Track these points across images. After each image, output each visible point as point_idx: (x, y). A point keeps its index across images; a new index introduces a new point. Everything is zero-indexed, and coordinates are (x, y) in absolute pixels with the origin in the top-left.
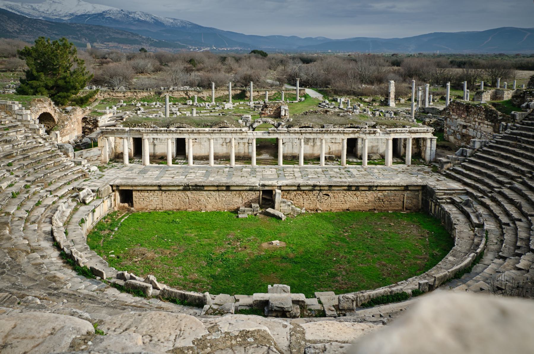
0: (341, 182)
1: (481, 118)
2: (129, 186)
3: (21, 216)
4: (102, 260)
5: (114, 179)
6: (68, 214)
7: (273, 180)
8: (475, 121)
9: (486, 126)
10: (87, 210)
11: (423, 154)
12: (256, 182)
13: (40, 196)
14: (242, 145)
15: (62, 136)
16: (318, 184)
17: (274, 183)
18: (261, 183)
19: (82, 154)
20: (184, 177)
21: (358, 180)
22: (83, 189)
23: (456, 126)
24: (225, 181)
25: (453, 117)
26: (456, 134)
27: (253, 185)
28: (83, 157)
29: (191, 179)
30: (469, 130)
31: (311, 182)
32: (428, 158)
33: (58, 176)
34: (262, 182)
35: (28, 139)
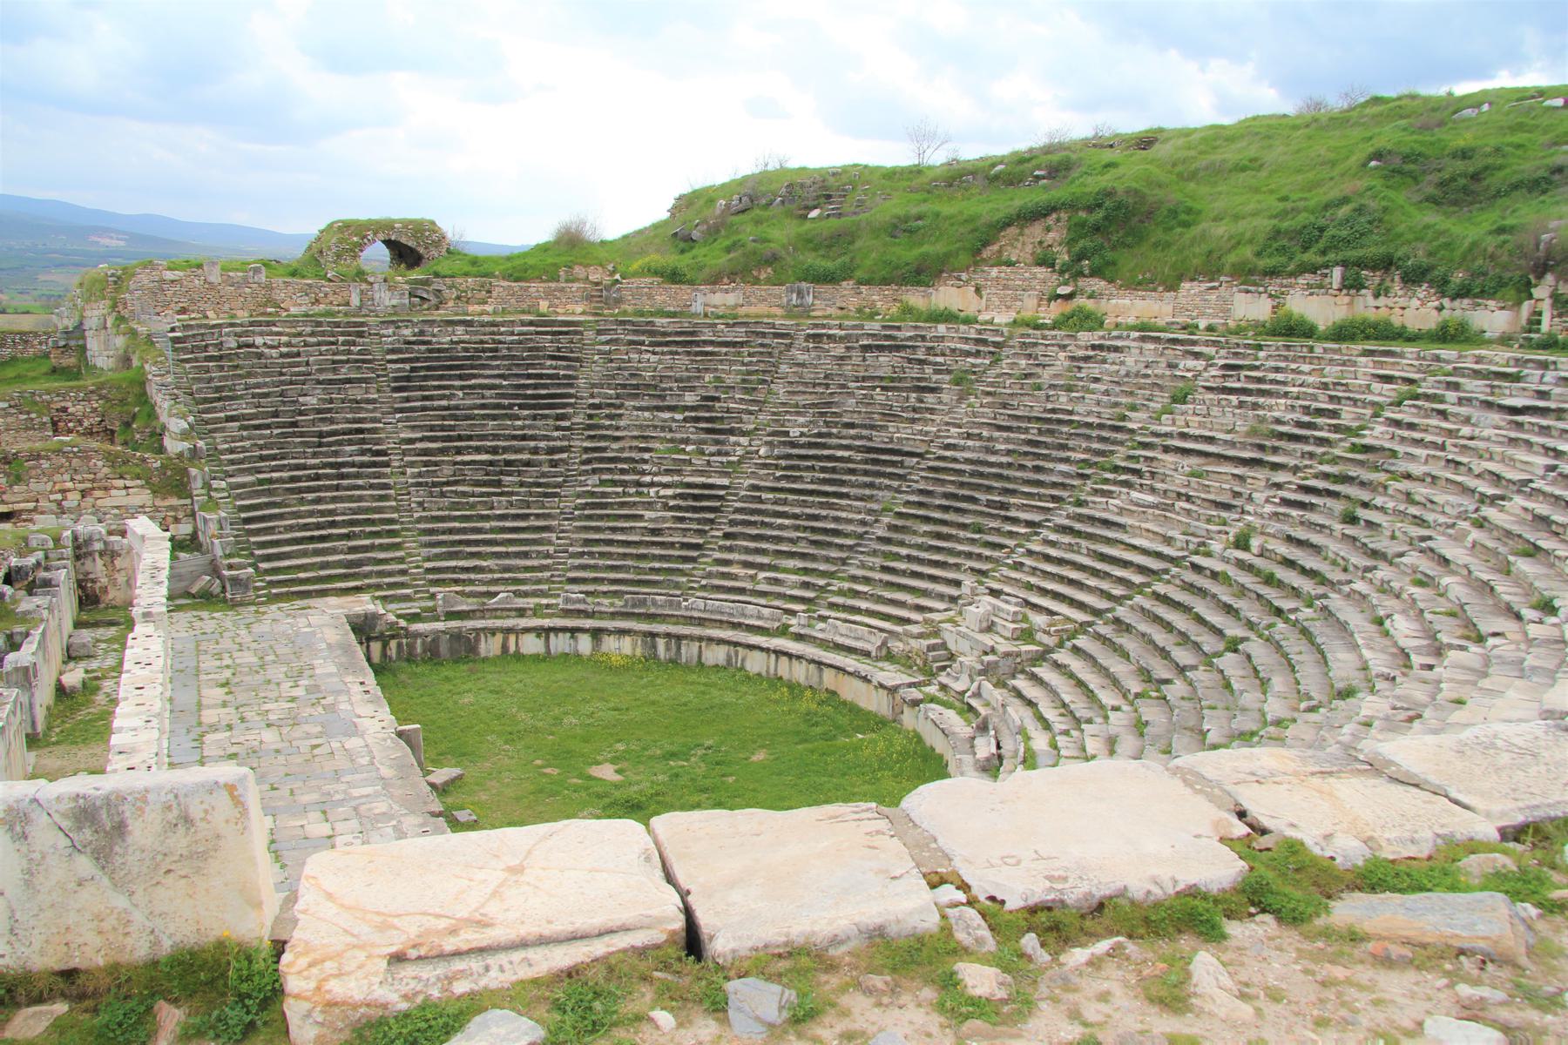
1: (92, 476)
8: (63, 491)
9: (124, 492)
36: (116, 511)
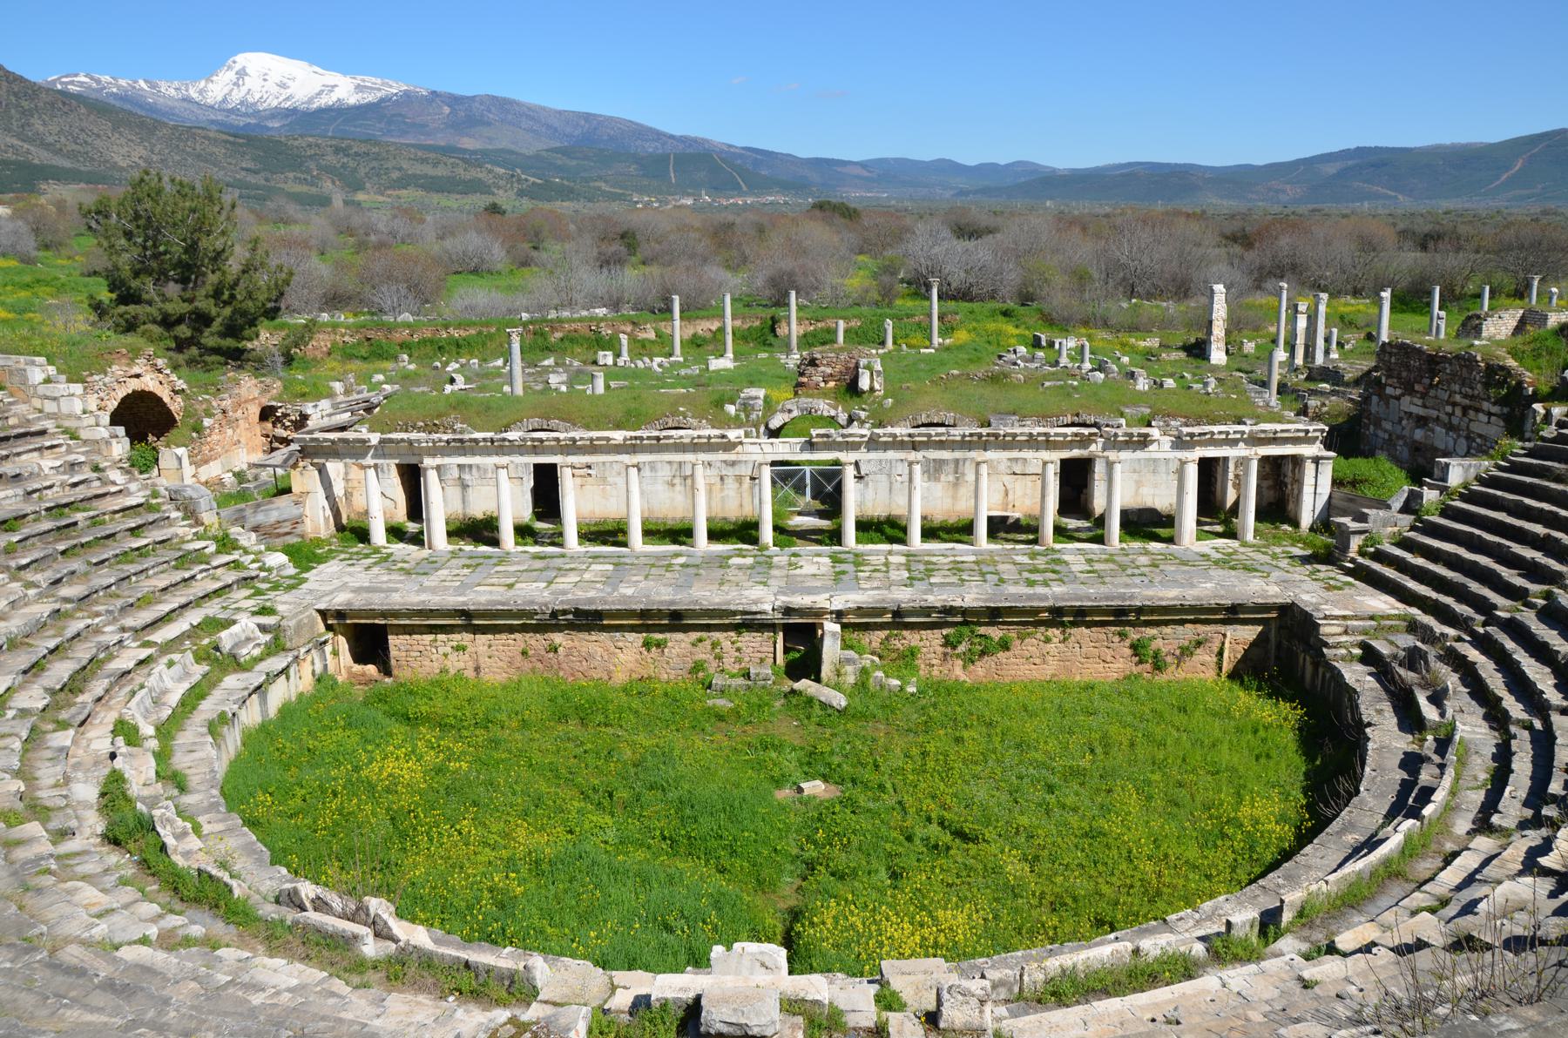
0: (1030, 597)
2: (372, 613)
3: (26, 705)
4: (253, 843)
5: (331, 592)
6: (174, 698)
7: (819, 593)
8: (1454, 404)
10: (241, 685)
11: (1291, 506)
12: (765, 598)
13: (99, 643)
14: (731, 483)
15: (197, 465)
16: (958, 603)
17: (821, 601)
18: (778, 603)
19: (244, 517)
20: (545, 584)
21: (1083, 590)
22: (234, 622)
23: (1396, 420)
24: (667, 598)
25: (1389, 390)
26: (1395, 445)
27: (754, 608)
28: (248, 526)
29: (564, 593)
30: (1433, 431)
31: (935, 599)
32: (1306, 519)
33: (162, 584)
34: (783, 600)
35: (78, 473)
36: (1478, 440)
